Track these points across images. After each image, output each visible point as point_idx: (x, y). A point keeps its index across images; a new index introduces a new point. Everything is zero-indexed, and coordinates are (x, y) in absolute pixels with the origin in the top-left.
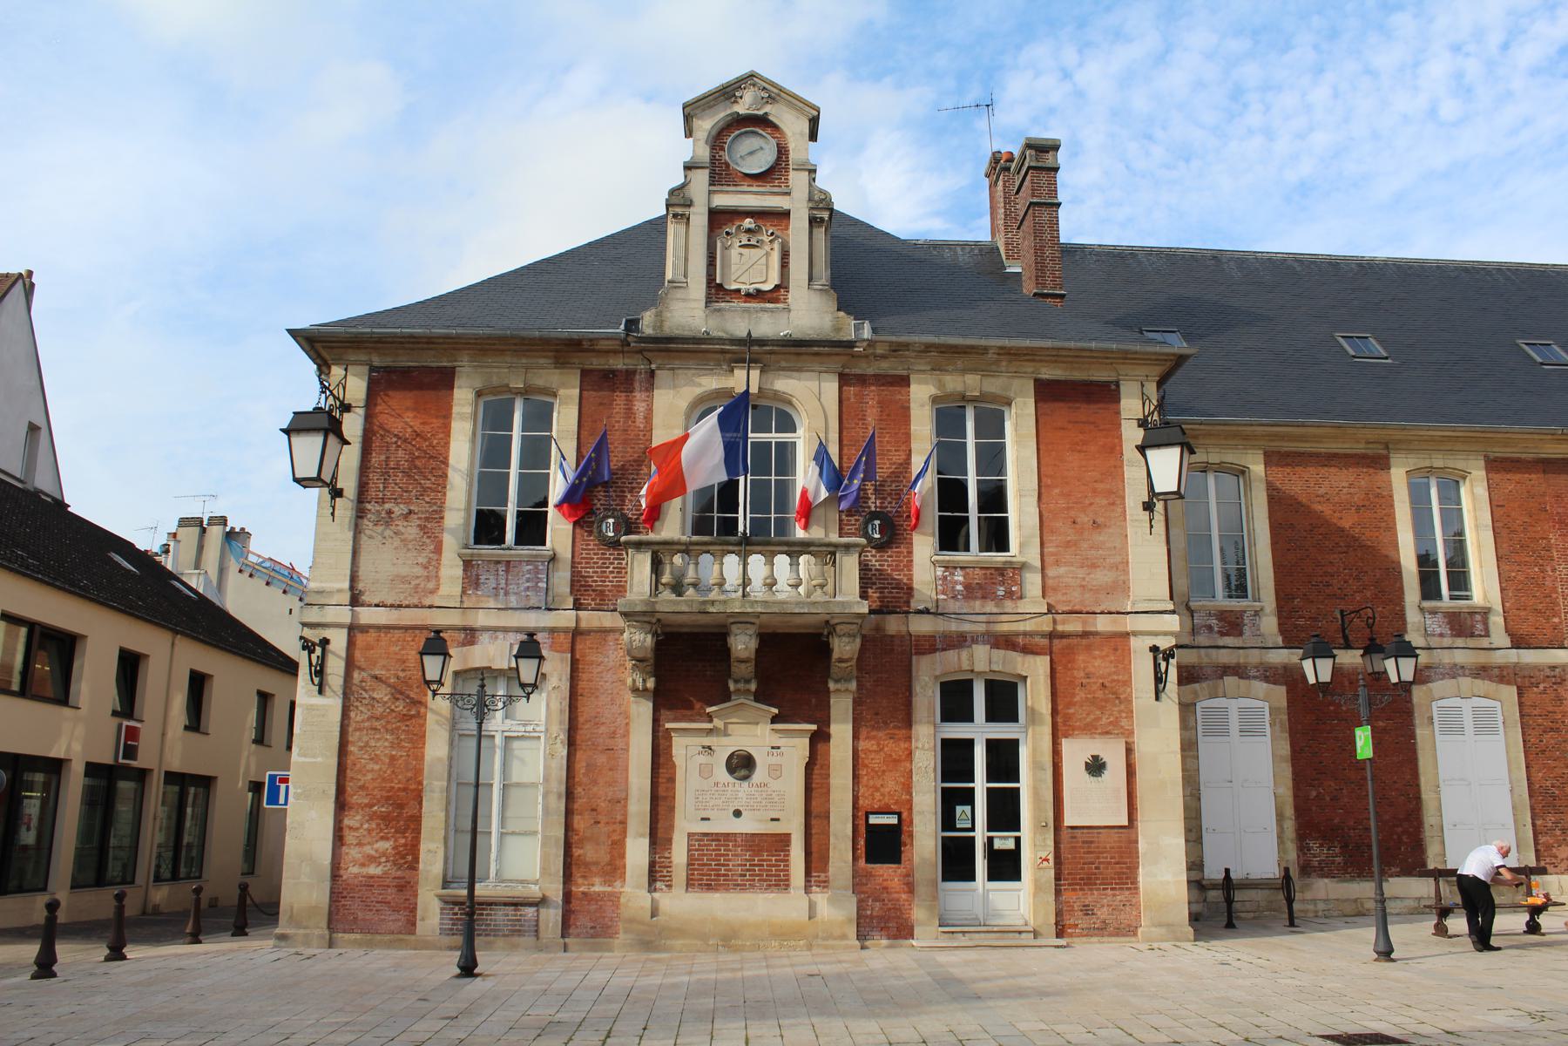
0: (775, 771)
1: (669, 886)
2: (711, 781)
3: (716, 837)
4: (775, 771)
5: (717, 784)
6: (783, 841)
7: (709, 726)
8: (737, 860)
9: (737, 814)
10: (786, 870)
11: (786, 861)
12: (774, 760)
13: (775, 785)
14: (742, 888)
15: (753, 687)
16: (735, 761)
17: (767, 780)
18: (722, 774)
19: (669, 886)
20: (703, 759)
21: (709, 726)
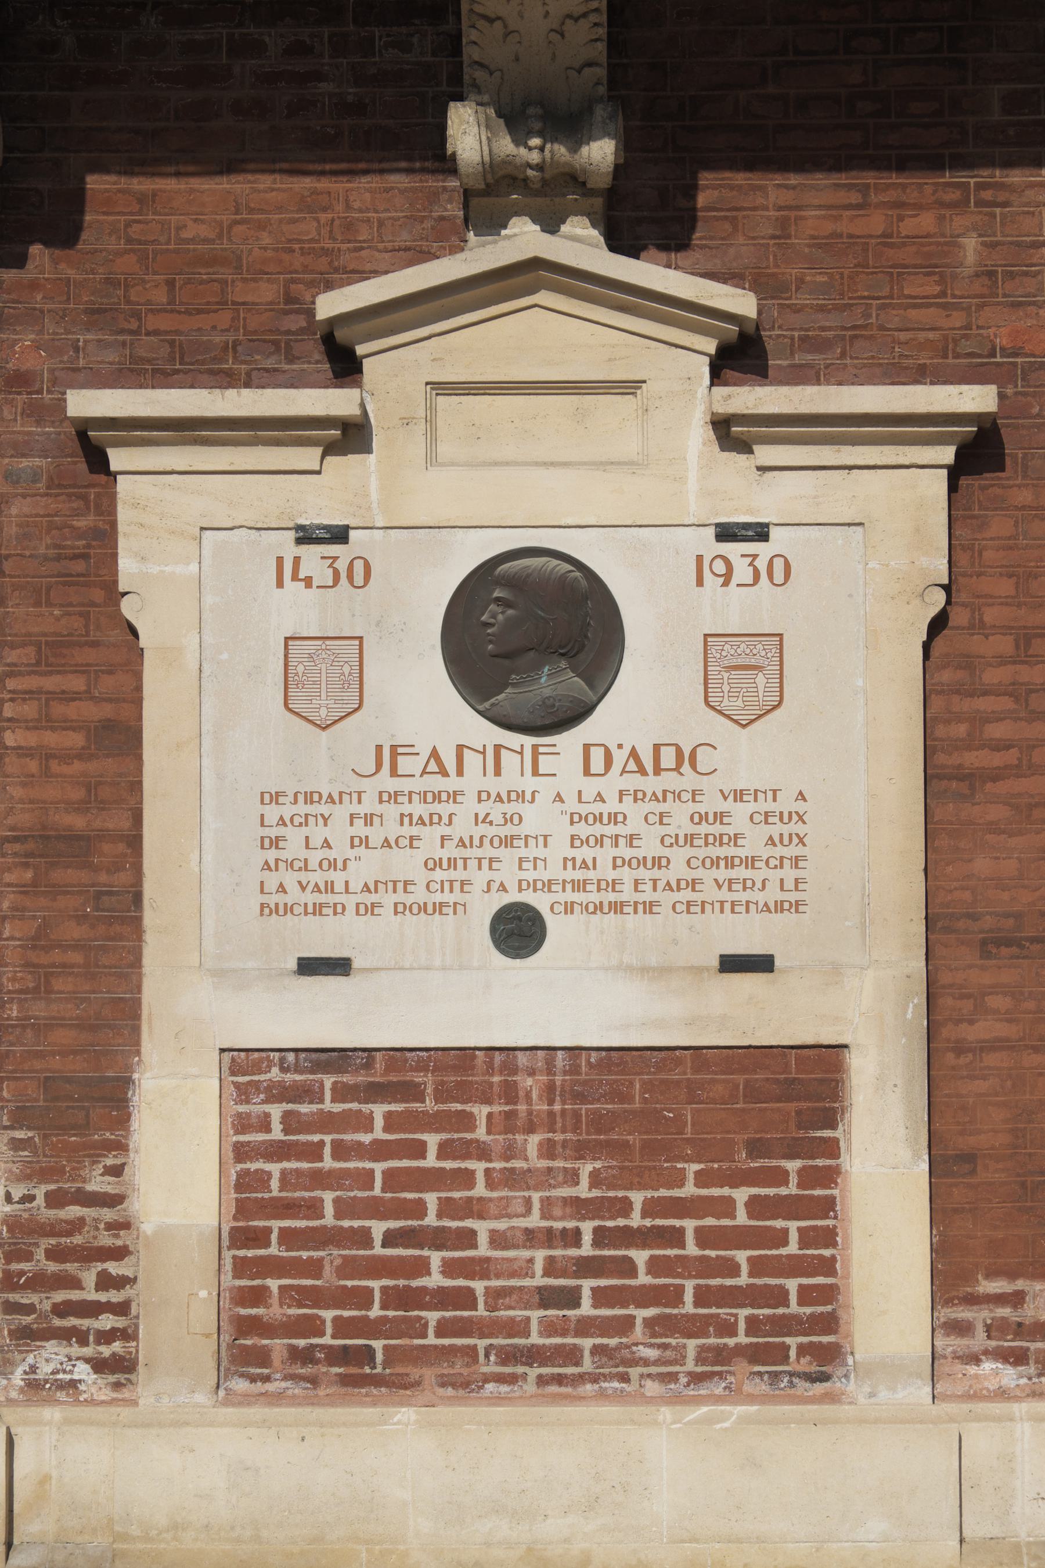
0: (745, 674)
1: (119, 1368)
2: (358, 737)
3: (387, 1073)
4: (745, 674)
5: (389, 757)
6: (804, 1087)
7: (336, 402)
8: (520, 1212)
9: (518, 931)
10: (822, 1261)
11: (819, 1206)
12: (736, 608)
13: (744, 758)
14: (556, 1370)
15: (600, 153)
16: (496, 616)
17: (699, 726)
18: (421, 698)
19: (119, 1368)
20: (298, 610)
21: (336, 402)
